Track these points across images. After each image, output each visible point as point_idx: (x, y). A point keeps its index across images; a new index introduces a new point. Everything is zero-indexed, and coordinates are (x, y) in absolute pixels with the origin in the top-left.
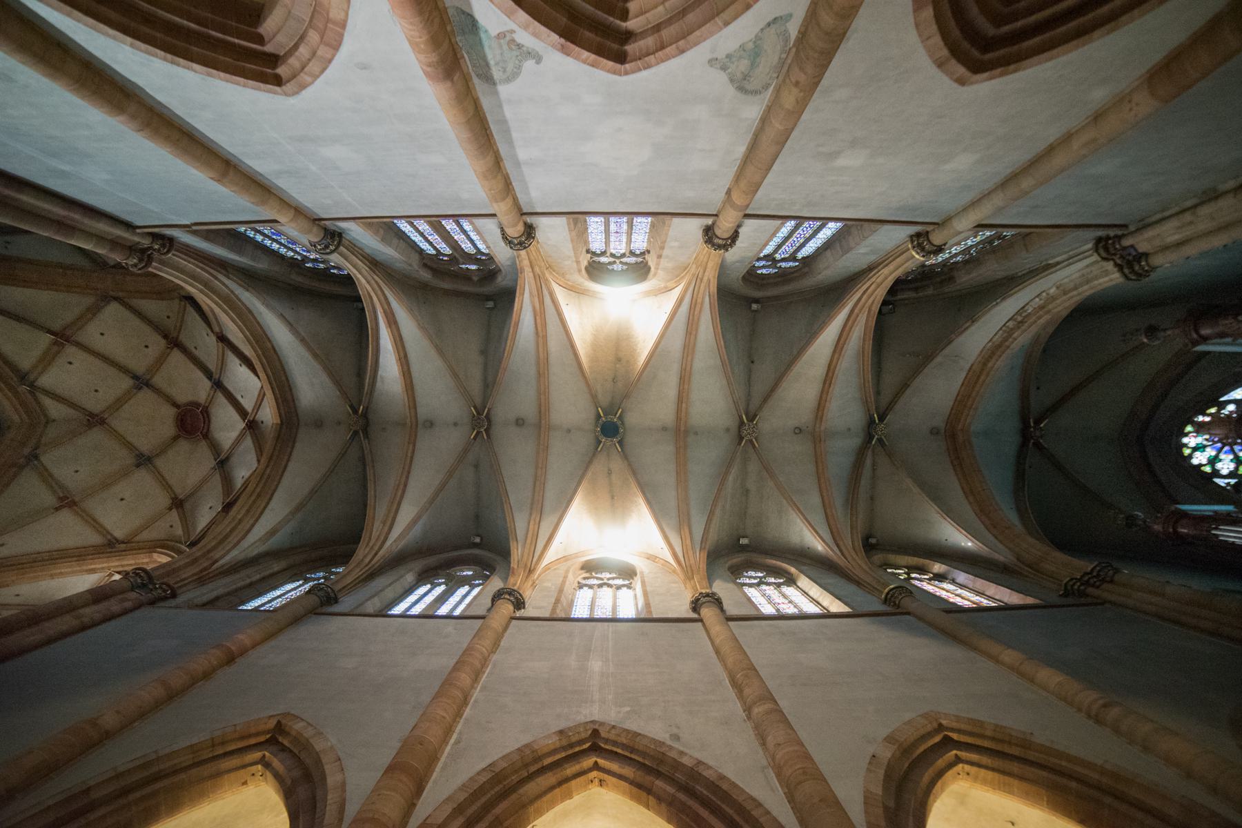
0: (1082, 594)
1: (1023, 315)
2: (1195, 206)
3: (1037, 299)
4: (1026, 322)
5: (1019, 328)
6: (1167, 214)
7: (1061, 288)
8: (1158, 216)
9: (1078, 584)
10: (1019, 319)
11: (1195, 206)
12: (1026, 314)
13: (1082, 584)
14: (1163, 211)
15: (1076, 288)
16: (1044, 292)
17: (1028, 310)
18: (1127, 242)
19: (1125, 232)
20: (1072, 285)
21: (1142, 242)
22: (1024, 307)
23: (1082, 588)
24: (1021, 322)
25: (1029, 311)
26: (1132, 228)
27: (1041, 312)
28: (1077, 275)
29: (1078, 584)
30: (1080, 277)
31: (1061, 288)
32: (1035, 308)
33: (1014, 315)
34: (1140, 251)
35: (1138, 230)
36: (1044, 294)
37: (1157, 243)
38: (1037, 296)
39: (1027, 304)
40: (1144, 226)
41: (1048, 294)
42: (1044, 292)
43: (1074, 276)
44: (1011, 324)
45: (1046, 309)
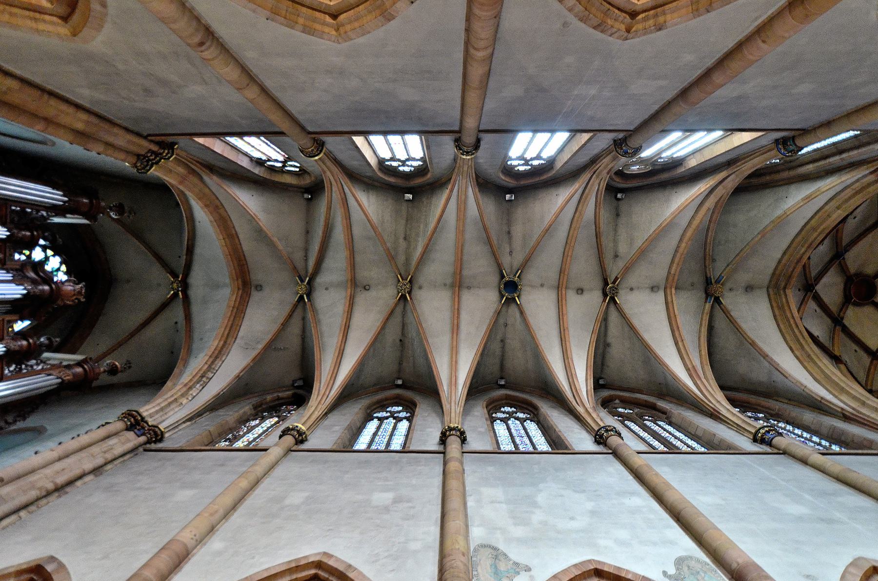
1: (202, 382)
3: (194, 394)
5: (204, 372)
6: (121, 459)
10: (204, 379)
14: (124, 461)
16: (190, 401)
18: (143, 439)
19: (145, 446)
20: (172, 406)
24: (202, 376)
25: (198, 385)
26: (141, 449)
33: (209, 381)
34: (132, 433)
38: (194, 397)
40: (133, 450)
41: (187, 399)
42: (190, 401)
44: (210, 375)
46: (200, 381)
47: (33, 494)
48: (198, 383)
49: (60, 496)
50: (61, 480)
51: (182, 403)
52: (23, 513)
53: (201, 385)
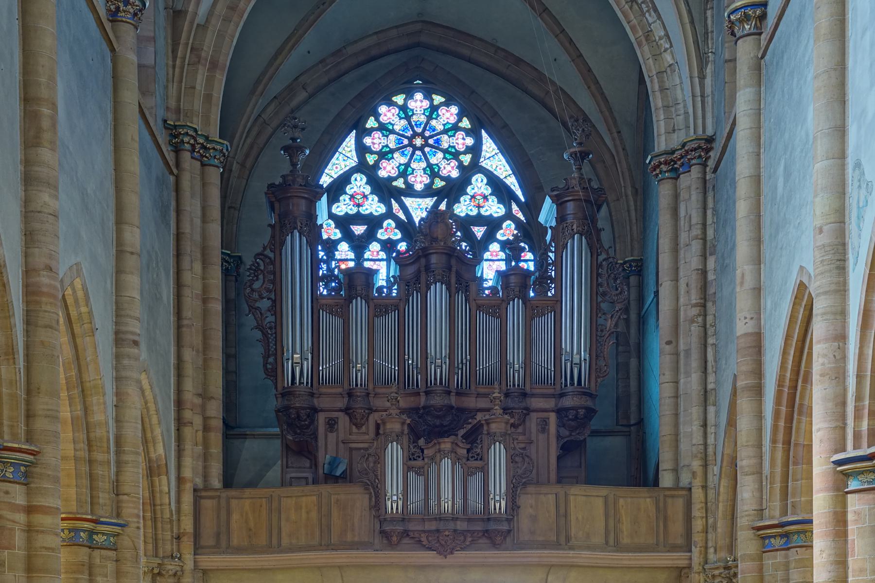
0: (177, 150)
1: (644, 6)
2: (704, 239)
3: (662, 33)
4: (631, 8)
7: (668, 70)
8: (710, 204)
9: (192, 141)
11: (704, 239)
12: (645, 9)
13: (193, 146)
14: (714, 209)
15: (663, 89)
16: (671, 46)
17: (650, 15)
18: (695, 171)
19: (708, 169)
21: (690, 180)
22: (656, 10)
23: (187, 146)
25: (647, 15)
27: (641, 33)
28: (680, 96)
29: (192, 141)
30: (676, 99)
31: (668, 70)
32: (650, 25)
35: (705, 181)
36: (668, 46)
37: (683, 195)
38: (667, 35)
39: (659, 17)
41: (665, 50)
42: (671, 46)
43: (679, 92)
45: (644, 42)
46: (641, 8)
47: (695, 329)
48: (643, 15)
49: (714, 302)
50: (695, 298)
51: (670, 66)
52: (711, 341)
53: (648, 11)
